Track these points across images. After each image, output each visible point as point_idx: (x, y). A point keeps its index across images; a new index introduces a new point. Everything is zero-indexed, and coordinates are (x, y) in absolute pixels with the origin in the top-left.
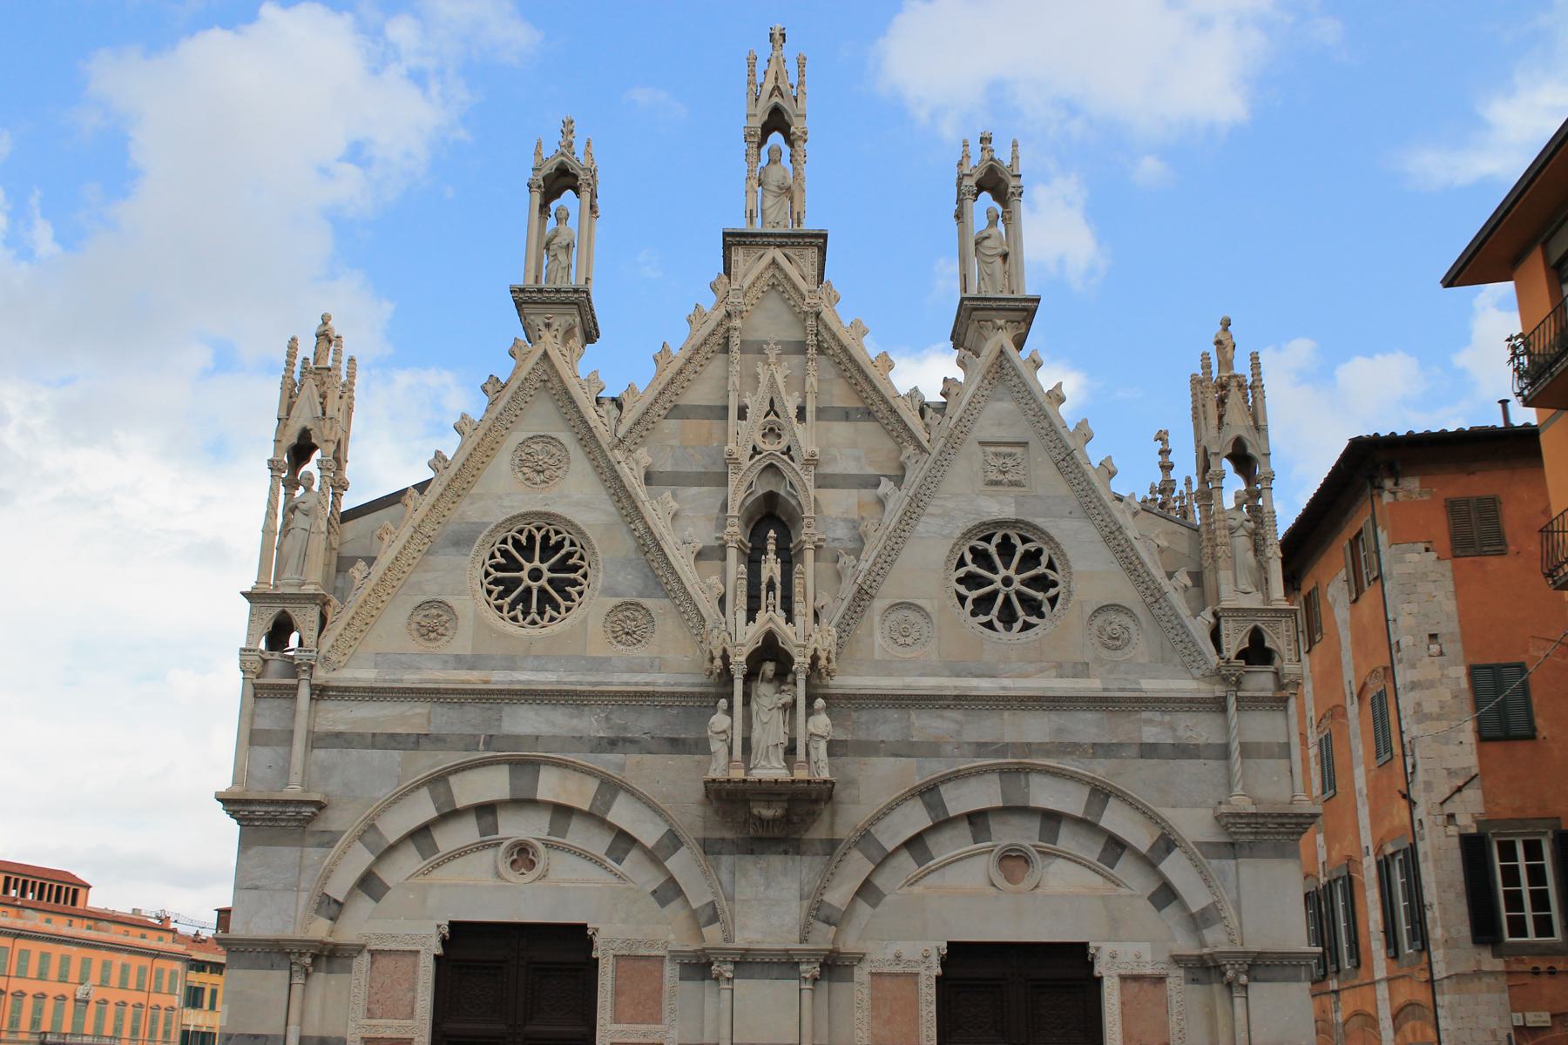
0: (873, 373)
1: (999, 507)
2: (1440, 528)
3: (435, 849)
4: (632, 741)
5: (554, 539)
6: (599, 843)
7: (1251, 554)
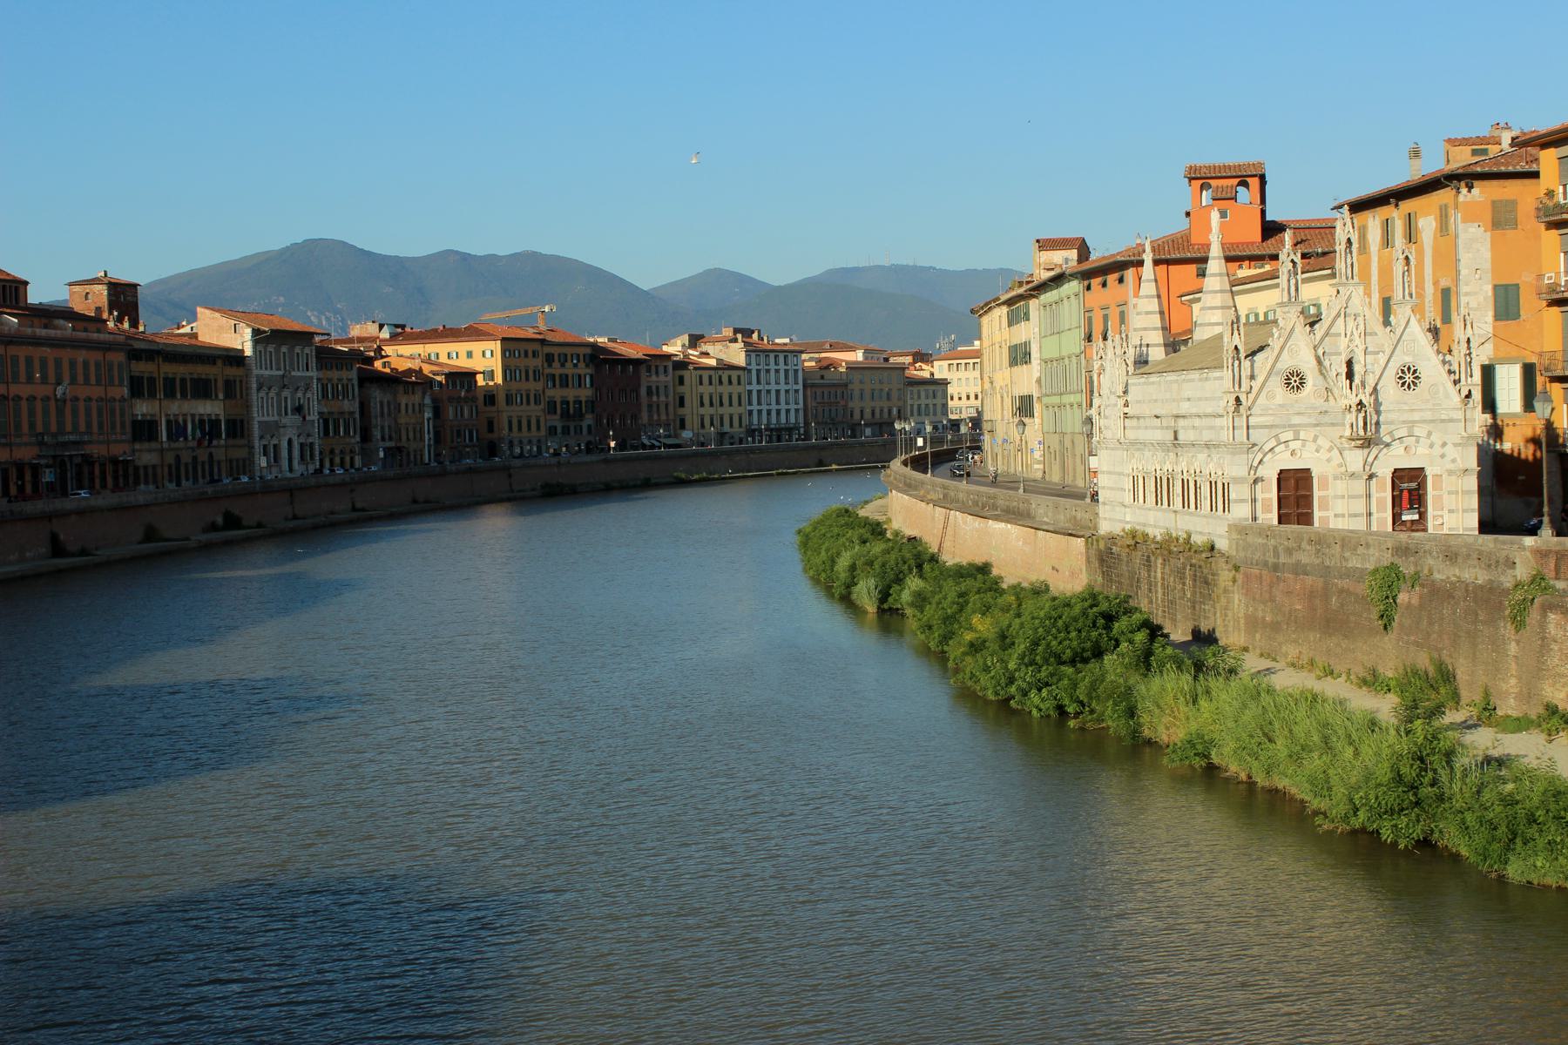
1: (1408, 360)
2: (1488, 216)
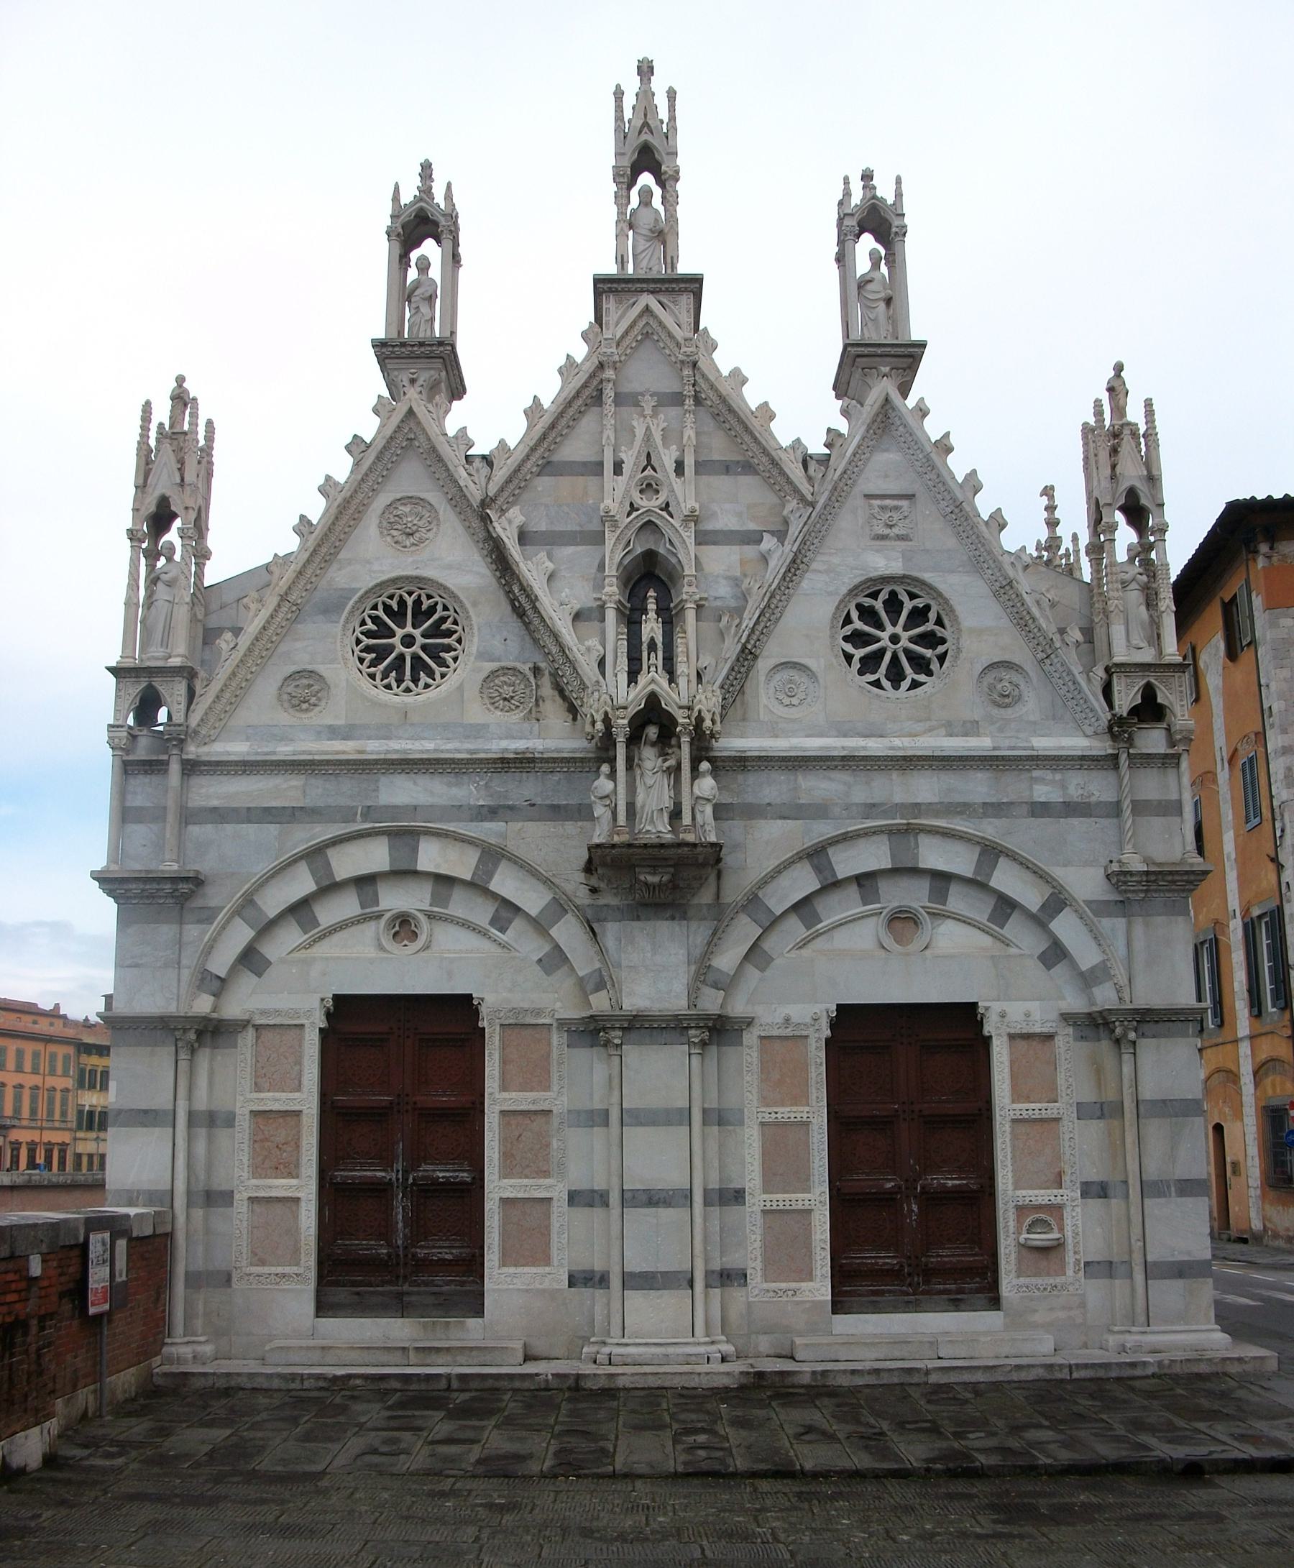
0: (755, 424)
1: (885, 563)
3: (315, 923)
4: (511, 808)
5: (426, 604)
6: (482, 913)
7: (1143, 608)
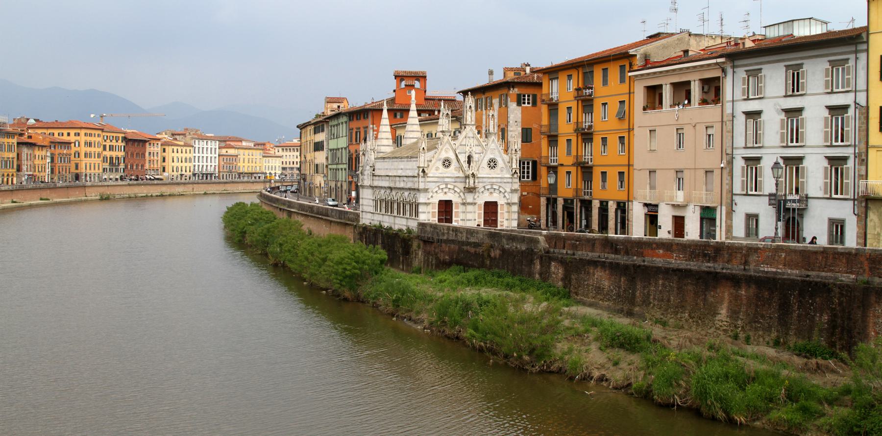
1: (492, 156)
